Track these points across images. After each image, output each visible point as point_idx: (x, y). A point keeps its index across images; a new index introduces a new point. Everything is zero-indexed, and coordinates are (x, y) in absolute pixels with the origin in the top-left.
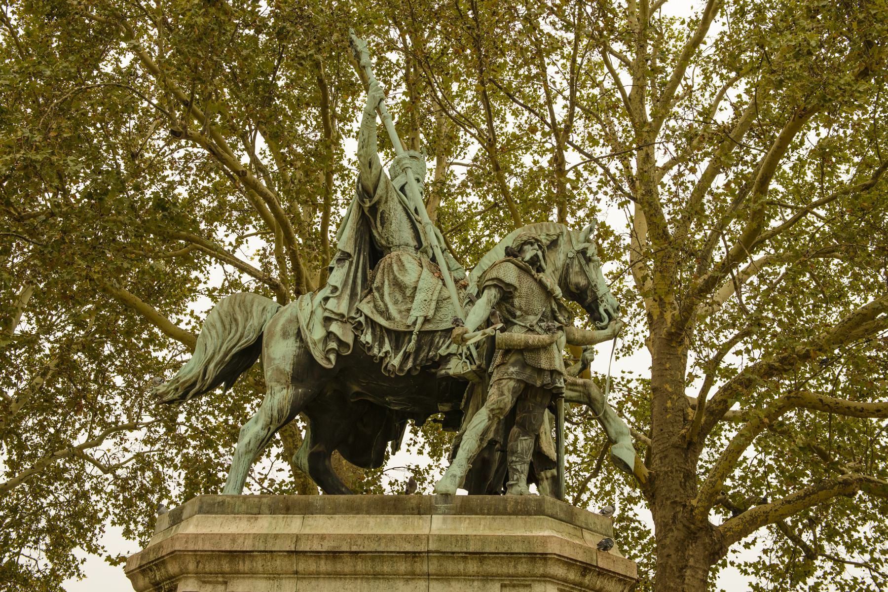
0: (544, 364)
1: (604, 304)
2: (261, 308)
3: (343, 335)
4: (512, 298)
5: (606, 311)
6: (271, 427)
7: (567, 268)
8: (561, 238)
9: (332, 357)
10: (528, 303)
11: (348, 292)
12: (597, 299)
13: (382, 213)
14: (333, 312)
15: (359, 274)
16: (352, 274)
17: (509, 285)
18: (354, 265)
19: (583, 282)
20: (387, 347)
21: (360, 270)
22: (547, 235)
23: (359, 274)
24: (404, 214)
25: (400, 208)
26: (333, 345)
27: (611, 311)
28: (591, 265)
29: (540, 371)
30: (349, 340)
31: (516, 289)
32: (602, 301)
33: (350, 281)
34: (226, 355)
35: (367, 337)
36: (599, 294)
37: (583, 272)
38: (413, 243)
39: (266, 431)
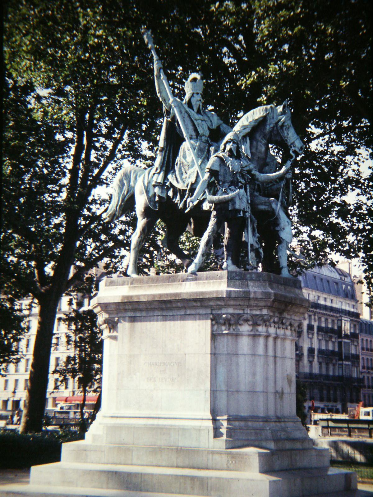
1: (293, 148)
2: (135, 175)
3: (162, 192)
9: (157, 205)
10: (225, 177)
11: (164, 168)
15: (171, 155)
16: (166, 158)
19: (279, 139)
20: (178, 198)
21: (171, 154)
23: (171, 155)
24: (188, 119)
25: (186, 116)
27: (297, 150)
28: (284, 128)
30: (164, 195)
33: (165, 162)
34: (123, 201)
35: (170, 194)
36: (289, 144)
37: (278, 134)
38: (194, 134)
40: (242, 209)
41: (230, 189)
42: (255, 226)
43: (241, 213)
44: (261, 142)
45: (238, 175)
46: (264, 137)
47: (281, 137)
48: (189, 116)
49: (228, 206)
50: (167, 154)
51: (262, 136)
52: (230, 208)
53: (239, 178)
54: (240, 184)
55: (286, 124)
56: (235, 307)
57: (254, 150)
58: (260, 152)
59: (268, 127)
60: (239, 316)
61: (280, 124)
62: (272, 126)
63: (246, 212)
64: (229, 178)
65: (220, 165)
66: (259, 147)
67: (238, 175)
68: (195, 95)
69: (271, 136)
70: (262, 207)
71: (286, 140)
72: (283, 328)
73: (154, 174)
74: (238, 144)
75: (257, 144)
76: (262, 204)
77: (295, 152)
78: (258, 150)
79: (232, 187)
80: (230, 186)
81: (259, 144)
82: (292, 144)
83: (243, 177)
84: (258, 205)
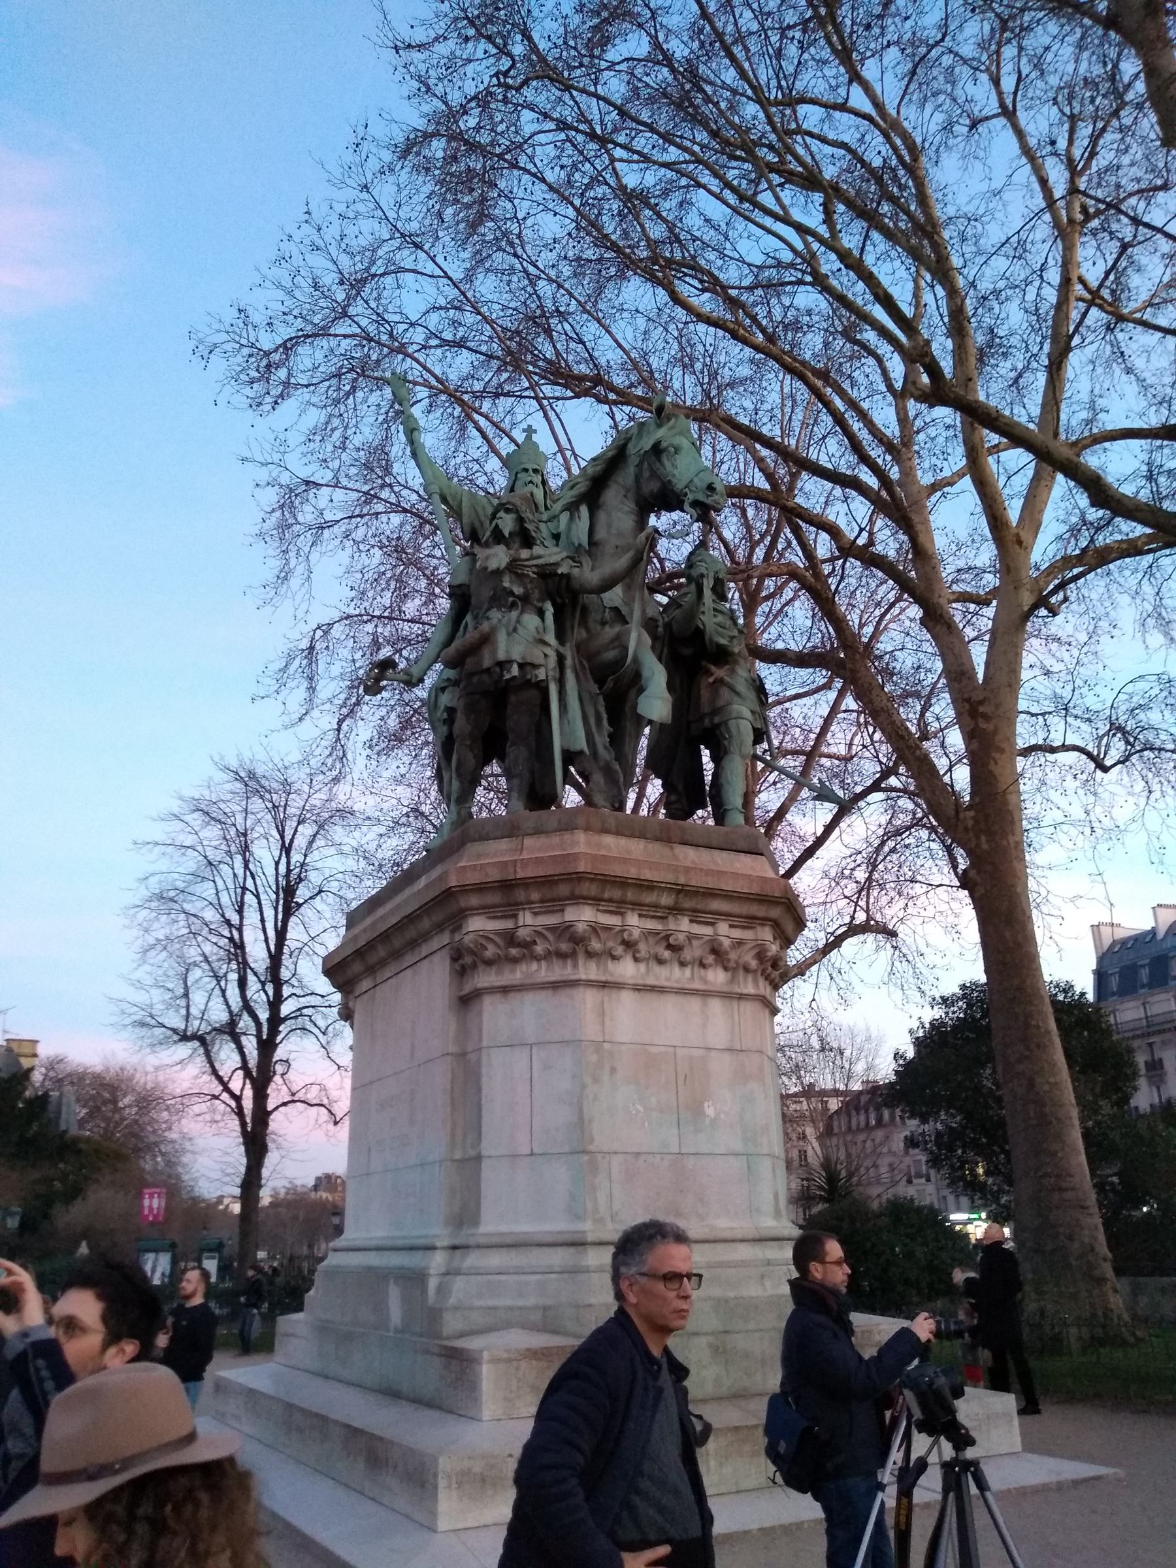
0: (487, 663)
4: (470, 597)
5: (696, 504)
7: (638, 478)
19: (653, 486)
26: (445, 716)
27: (701, 497)
29: (488, 670)
31: (468, 586)
37: (654, 474)
40: (516, 656)
42: (602, 709)
43: (515, 666)
47: (659, 478)
53: (506, 584)
55: (664, 445)
56: (487, 910)
57: (601, 534)
58: (620, 534)
60: (510, 938)
61: (648, 447)
62: (637, 461)
63: (535, 666)
64: (486, 593)
70: (610, 655)
72: (683, 964)
74: (517, 512)
76: (607, 648)
77: (696, 504)
78: (614, 531)
80: (489, 609)
83: (520, 577)
84: (599, 653)
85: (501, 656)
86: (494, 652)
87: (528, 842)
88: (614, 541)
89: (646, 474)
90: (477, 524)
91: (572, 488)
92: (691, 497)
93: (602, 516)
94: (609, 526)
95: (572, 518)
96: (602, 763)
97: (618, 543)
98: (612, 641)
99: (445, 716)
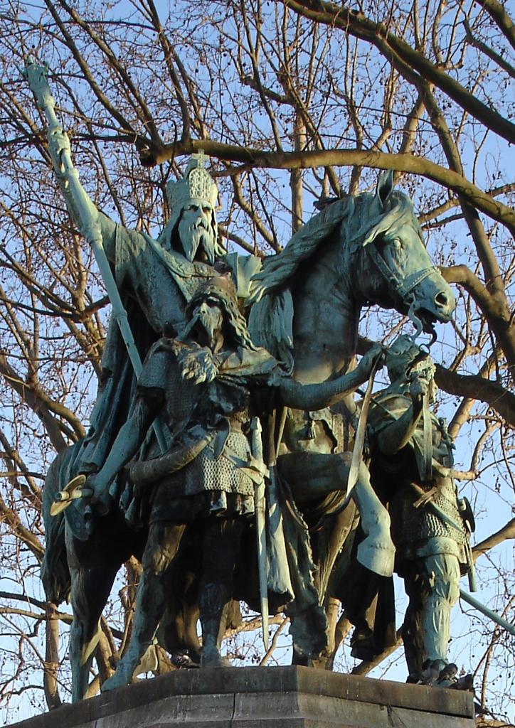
0: (190, 489)
4: (164, 402)
6: (82, 621)
7: (354, 267)
8: (346, 227)
9: (87, 526)
12: (403, 300)
13: (140, 289)
14: (88, 464)
17: (152, 389)
18: (122, 378)
19: (374, 282)
22: (304, 239)
26: (87, 510)
29: (191, 498)
32: (411, 300)
33: (114, 407)
37: (374, 268)
39: (80, 628)
41: (190, 435)
44: (330, 301)
45: (213, 391)
46: (337, 286)
48: (167, 270)
49: (184, 483)
50: (120, 385)
51: (330, 286)
52: (190, 489)
53: (214, 398)
54: (218, 416)
57: (307, 327)
58: (329, 331)
59: (346, 255)
62: (354, 248)
64: (189, 406)
65: (167, 373)
66: (324, 317)
67: (213, 391)
68: (186, 213)
69: (354, 277)
71: (394, 281)
73: (86, 444)
74: (221, 306)
75: (317, 307)
78: (321, 326)
79: (197, 430)
80: (190, 425)
81: (324, 306)
82: (413, 290)
85: (209, 485)
86: (200, 477)
87: (241, 700)
88: (322, 338)
89: (365, 266)
90: (132, 270)
91: (274, 269)
92: (417, 304)
93: (309, 306)
94: (317, 320)
95: (272, 306)
96: (304, 606)
97: (327, 341)
98: (324, 468)
99: (87, 510)
